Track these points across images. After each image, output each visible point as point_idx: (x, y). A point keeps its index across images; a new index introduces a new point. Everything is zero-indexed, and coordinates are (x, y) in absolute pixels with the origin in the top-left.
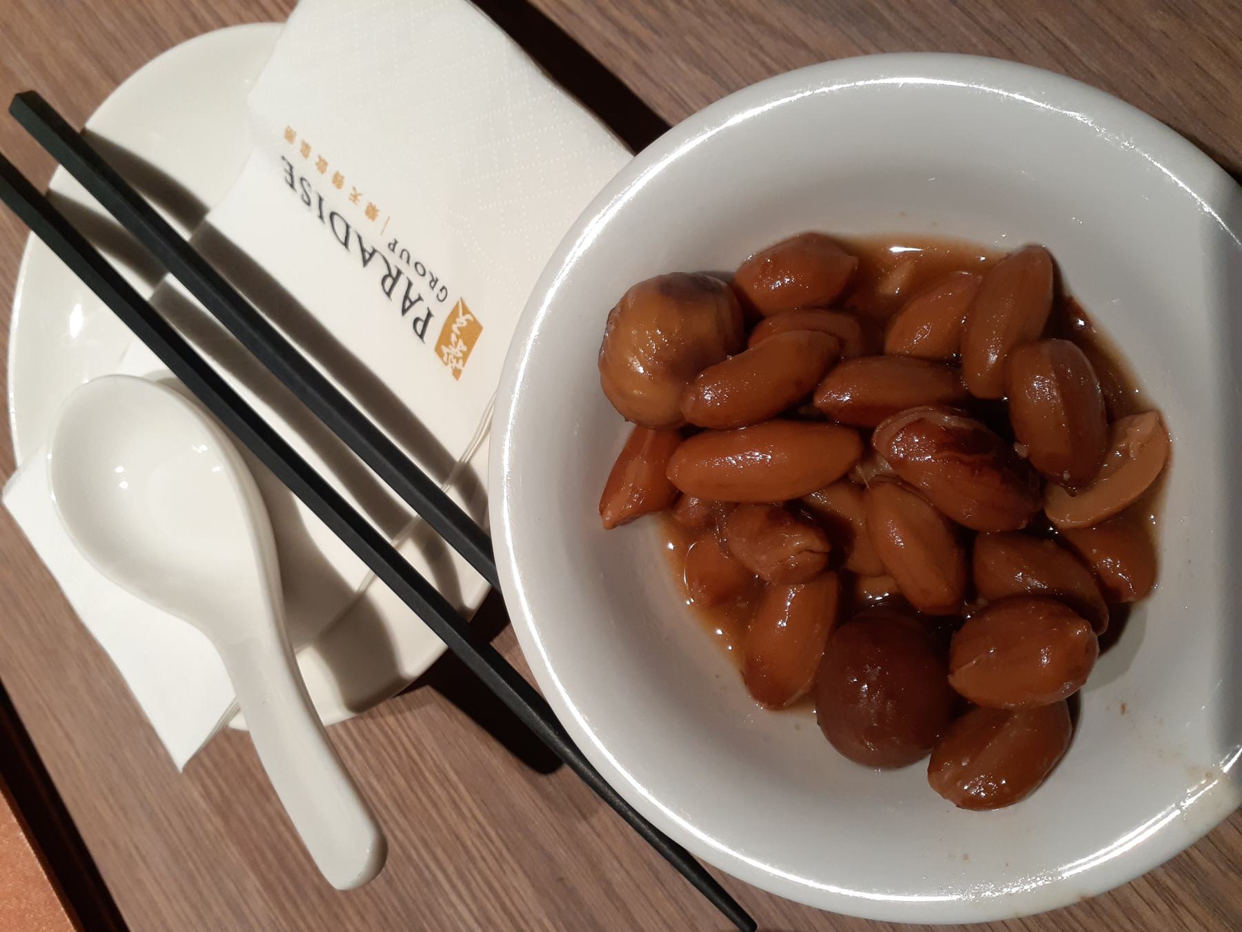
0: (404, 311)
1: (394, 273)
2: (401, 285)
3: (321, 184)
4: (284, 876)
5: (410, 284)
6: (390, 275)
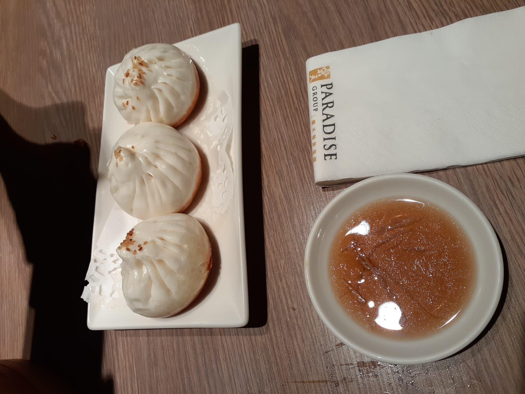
0: (331, 94)
1: (325, 106)
2: (326, 100)
5: (323, 99)
6: (327, 106)
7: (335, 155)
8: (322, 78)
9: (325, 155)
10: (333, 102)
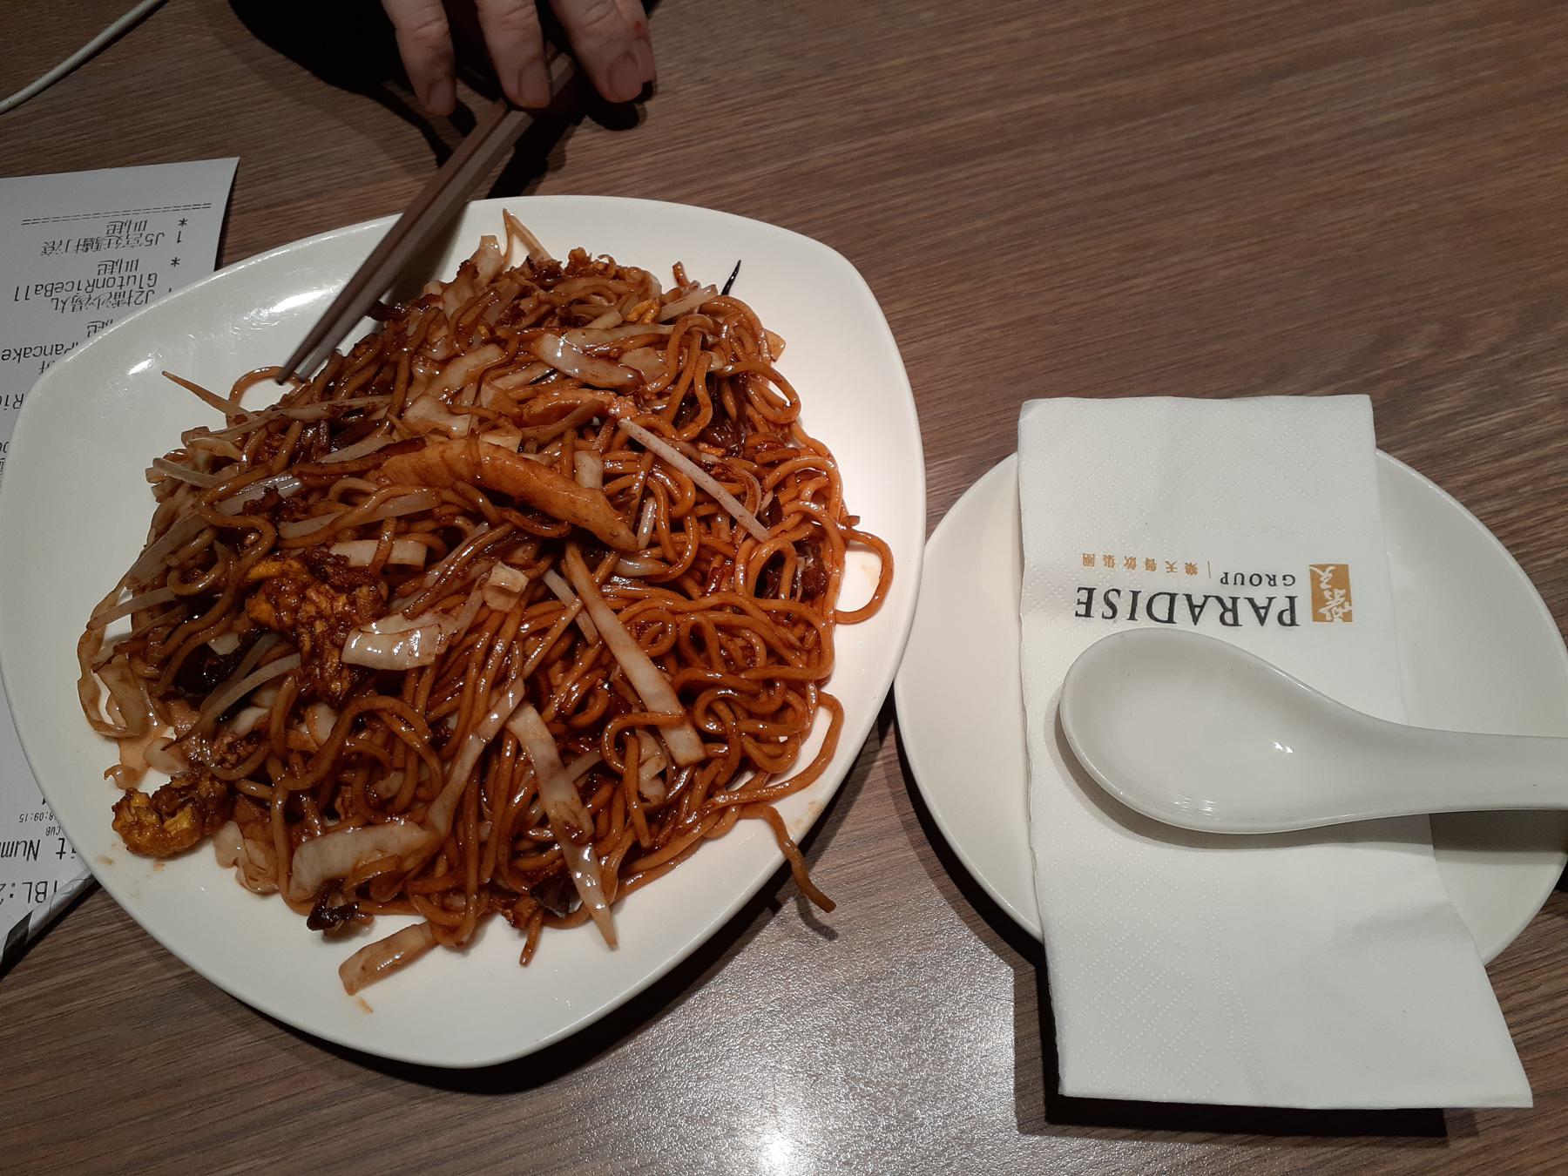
0: (1262, 620)
2: (1243, 607)
5: (1251, 601)
7: (1088, 614)
8: (1318, 600)
9: (1090, 591)
10: (1236, 623)
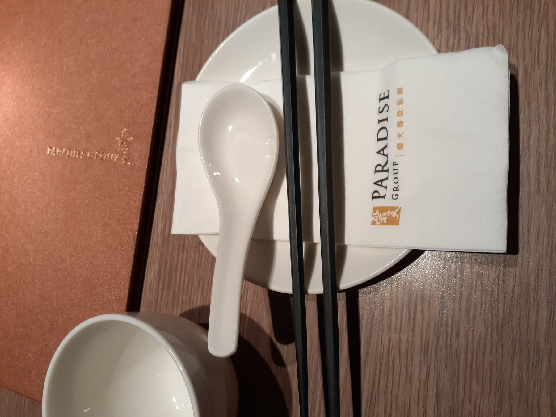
0: (376, 183)
1: (385, 168)
2: (383, 175)
3: (392, 114)
4: (167, 277)
5: (387, 179)
6: (383, 167)
8: (382, 210)
10: (376, 171)
